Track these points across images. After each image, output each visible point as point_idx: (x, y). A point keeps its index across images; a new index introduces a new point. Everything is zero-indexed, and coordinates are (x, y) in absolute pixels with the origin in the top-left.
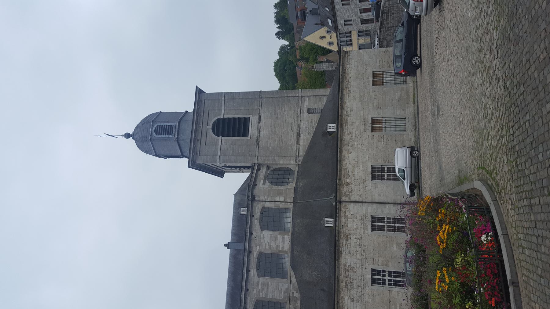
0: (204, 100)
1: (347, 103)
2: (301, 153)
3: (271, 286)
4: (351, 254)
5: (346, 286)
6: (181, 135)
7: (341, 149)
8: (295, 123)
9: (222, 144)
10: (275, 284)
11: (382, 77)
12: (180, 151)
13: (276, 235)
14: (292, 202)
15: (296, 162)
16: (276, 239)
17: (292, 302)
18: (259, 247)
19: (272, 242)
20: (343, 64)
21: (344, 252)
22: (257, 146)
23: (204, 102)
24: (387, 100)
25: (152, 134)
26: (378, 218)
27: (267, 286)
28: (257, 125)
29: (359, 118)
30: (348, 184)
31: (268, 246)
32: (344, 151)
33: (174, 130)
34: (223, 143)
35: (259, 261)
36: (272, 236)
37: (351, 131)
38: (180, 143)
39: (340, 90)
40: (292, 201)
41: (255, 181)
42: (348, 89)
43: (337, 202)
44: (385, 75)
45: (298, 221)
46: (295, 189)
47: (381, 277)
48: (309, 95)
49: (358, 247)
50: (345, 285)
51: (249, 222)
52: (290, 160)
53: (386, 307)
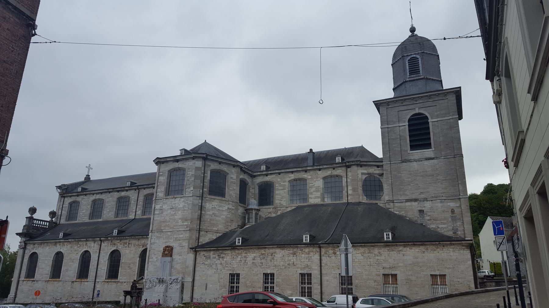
0: (447, 98)
1: (411, 250)
2: (397, 205)
3: (283, 192)
4: (283, 258)
5: (262, 254)
6: (410, 84)
7: (365, 246)
8: (429, 195)
9: (400, 127)
10: (285, 195)
11: (441, 283)
12: (396, 86)
13: (320, 191)
14: (348, 202)
15: (387, 201)
16: (317, 191)
17: (274, 210)
18: (310, 178)
19: (315, 188)
20: (453, 244)
21: (284, 252)
22: (400, 161)
23: (445, 98)
24: (416, 288)
25: (409, 55)
26: (311, 279)
27: (284, 189)
28: (424, 157)
29: (396, 262)
30: (335, 253)
31: (312, 186)
32: (363, 249)
33: (415, 76)
34: (402, 128)
35: (300, 179)
36: (319, 188)
37: (383, 255)
38: (403, 85)
39: (422, 243)
40: (349, 201)
41: (365, 165)
42: (426, 251)
43: (318, 245)
44: (443, 286)
45: (330, 209)
46: (359, 203)
47: (269, 281)
48: (462, 206)
49: (288, 263)
50: (263, 253)
51: (328, 167)
53: (250, 284)
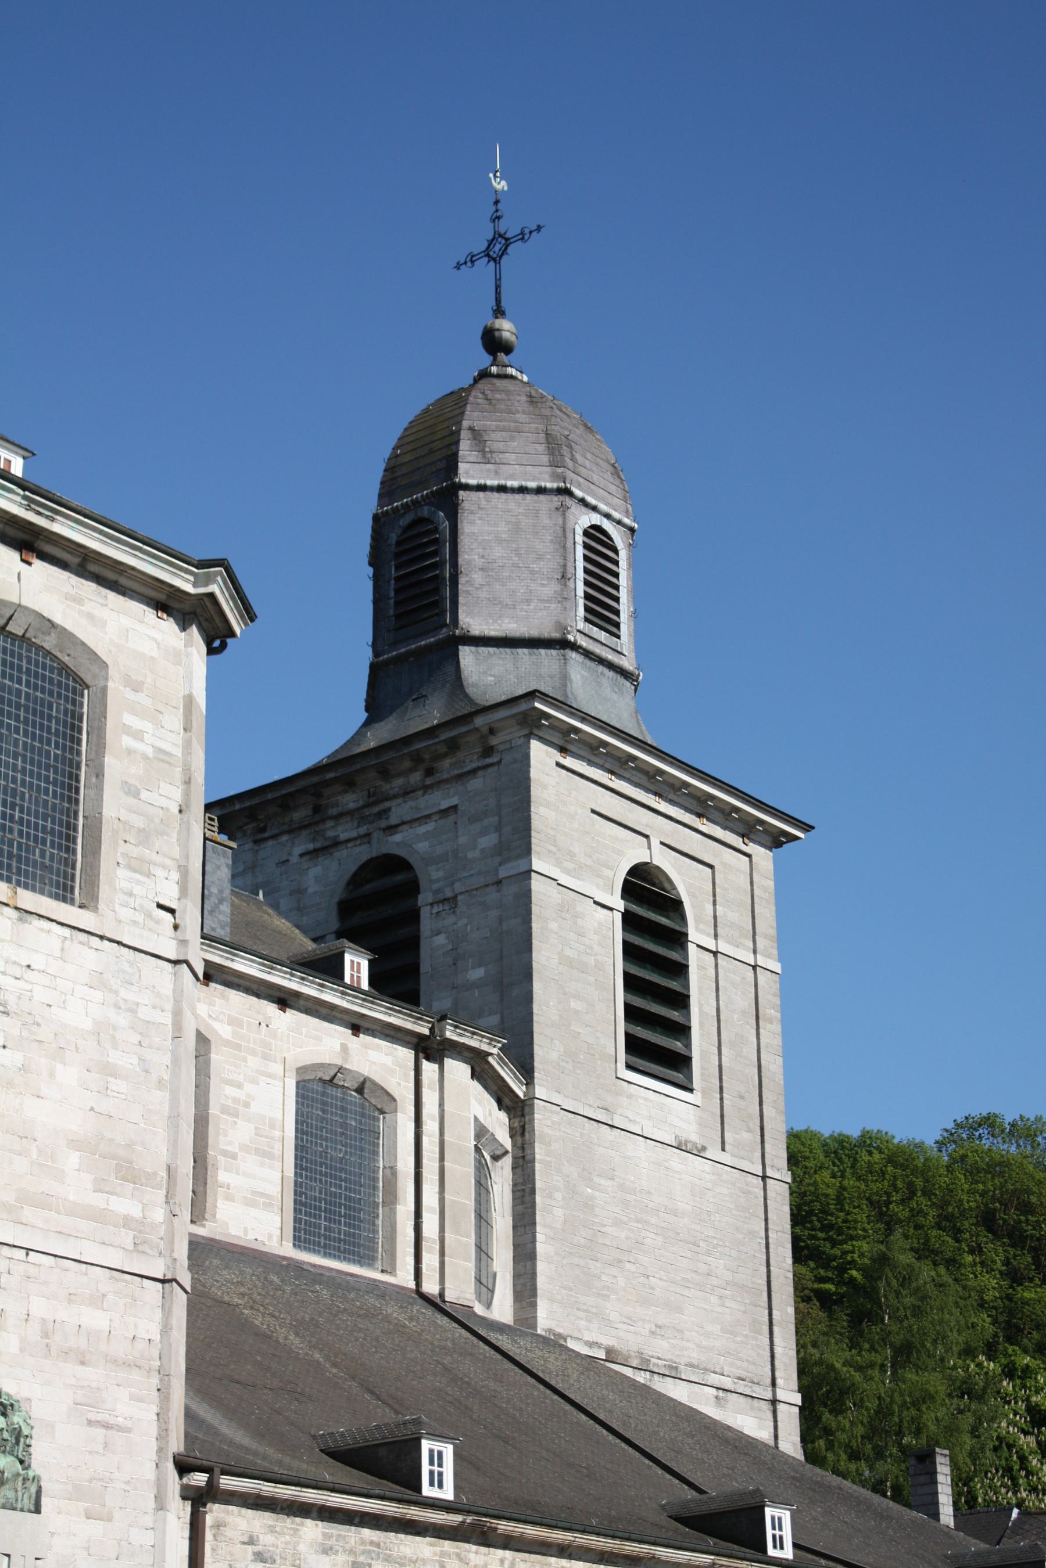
52: (552, 1300)
